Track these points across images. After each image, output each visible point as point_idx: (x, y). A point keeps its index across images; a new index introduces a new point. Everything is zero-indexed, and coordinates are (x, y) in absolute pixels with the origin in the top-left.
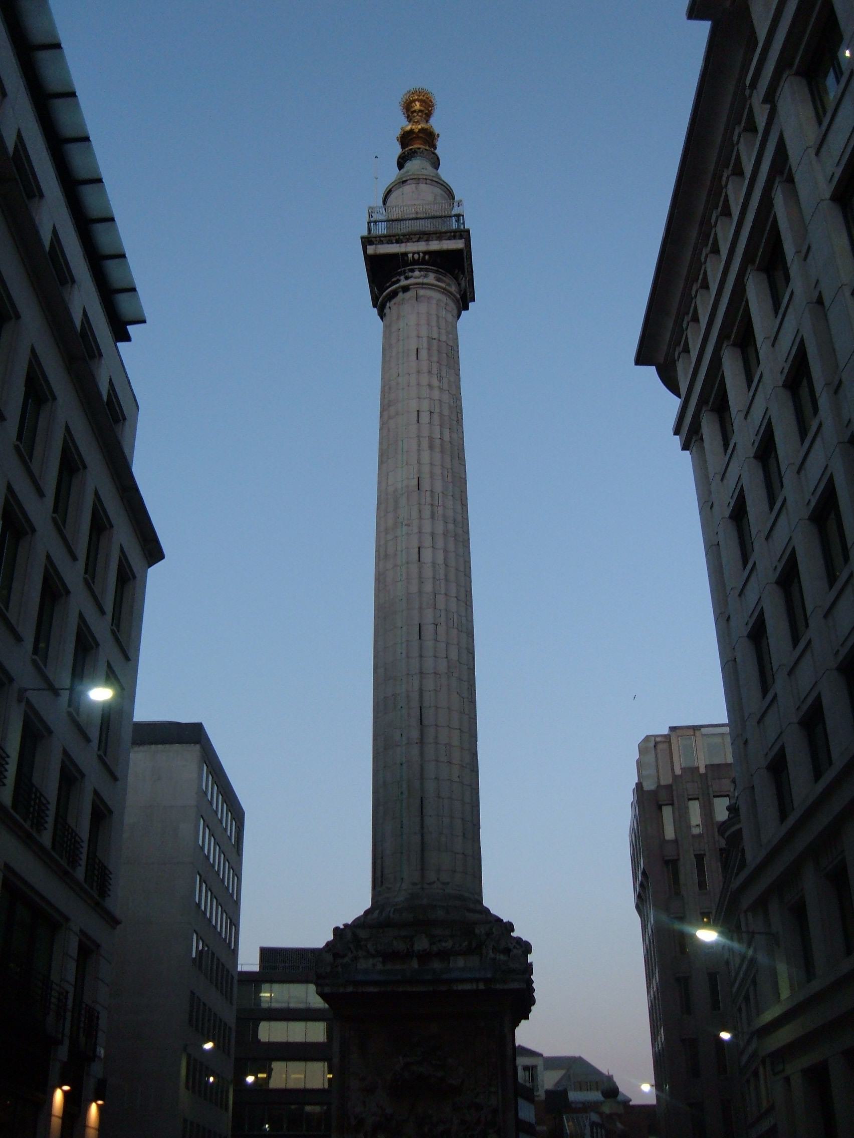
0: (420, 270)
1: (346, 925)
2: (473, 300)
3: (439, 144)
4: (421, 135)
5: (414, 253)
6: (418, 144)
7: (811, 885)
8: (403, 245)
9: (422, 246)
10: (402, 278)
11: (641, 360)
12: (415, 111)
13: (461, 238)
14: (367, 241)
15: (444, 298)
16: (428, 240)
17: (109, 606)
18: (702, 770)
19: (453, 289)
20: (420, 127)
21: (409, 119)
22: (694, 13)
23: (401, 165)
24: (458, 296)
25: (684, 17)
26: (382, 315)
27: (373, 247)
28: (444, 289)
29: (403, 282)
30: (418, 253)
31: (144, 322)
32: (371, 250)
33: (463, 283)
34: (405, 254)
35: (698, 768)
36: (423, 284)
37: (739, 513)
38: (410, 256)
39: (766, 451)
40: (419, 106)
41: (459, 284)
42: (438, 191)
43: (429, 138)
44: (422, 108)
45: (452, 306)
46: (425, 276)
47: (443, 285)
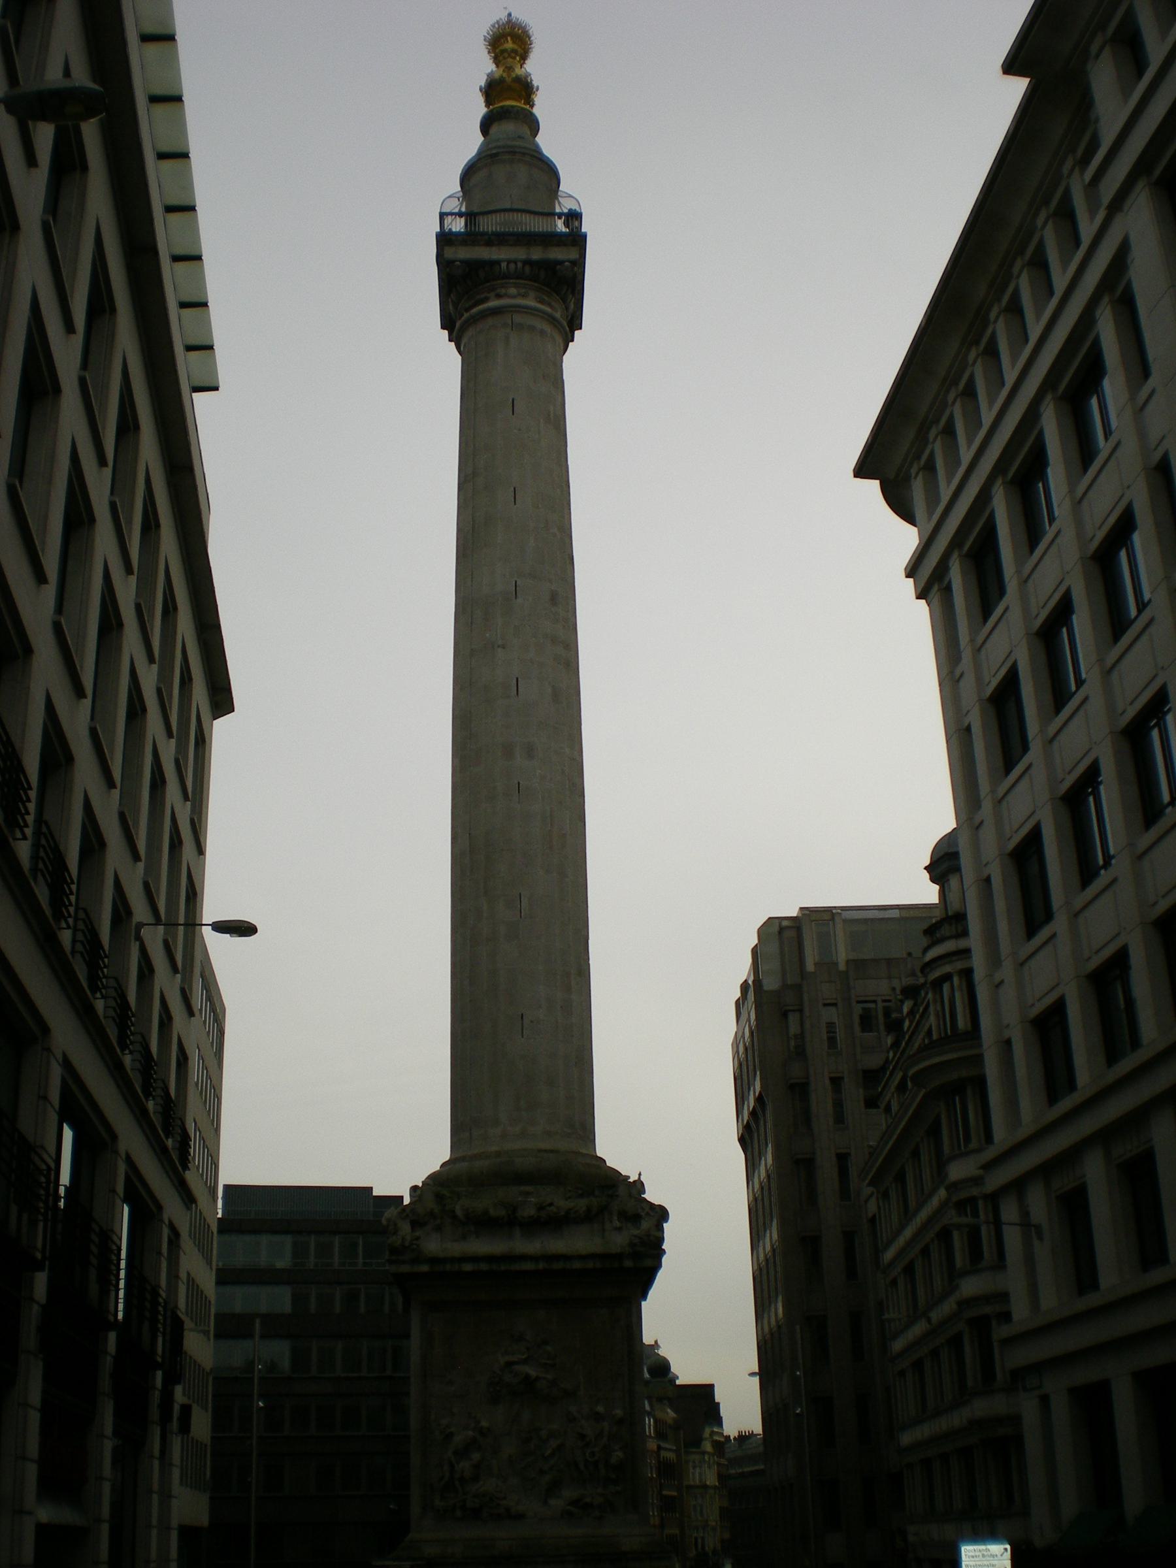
0: (516, 286)
5: (509, 262)
7: (1095, 1172)
9: (519, 253)
10: (492, 295)
11: (863, 470)
14: (445, 239)
15: (548, 328)
18: (842, 967)
21: (497, 60)
22: (1011, 67)
29: (493, 303)
31: (216, 389)
32: (450, 253)
35: (836, 964)
36: (519, 306)
37: (1004, 698)
38: (504, 265)
39: (1051, 631)
40: (510, 42)
41: (567, 308)
43: (526, 90)
44: (515, 47)
46: (524, 296)
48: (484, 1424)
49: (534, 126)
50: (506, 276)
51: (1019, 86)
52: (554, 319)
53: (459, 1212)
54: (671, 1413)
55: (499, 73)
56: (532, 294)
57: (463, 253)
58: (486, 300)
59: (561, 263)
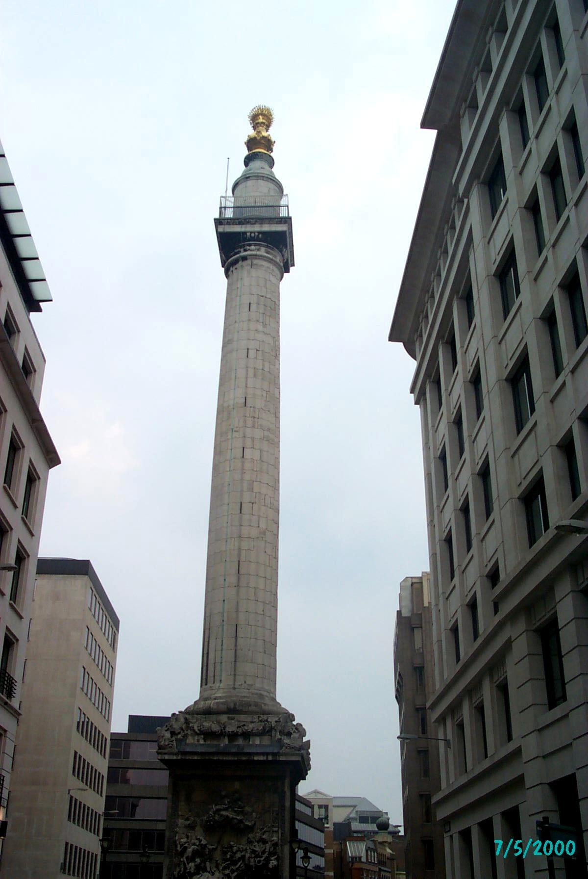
0: (255, 245)
1: (180, 712)
2: (293, 265)
3: (275, 148)
6: (259, 149)
11: (393, 338)
13: (285, 222)
14: (218, 222)
15: (271, 266)
16: (261, 223)
17: (20, 502)
19: (278, 259)
21: (254, 128)
22: (425, 124)
23: (246, 164)
24: (282, 264)
25: (419, 126)
26: (227, 276)
29: (243, 254)
32: (221, 229)
33: (286, 255)
34: (245, 233)
36: (256, 255)
40: (261, 119)
42: (272, 186)
43: (268, 144)
45: (277, 271)
48: (204, 842)
49: (271, 163)
51: (432, 134)
53: (196, 728)
54: (389, 851)
56: (263, 249)
58: (240, 252)
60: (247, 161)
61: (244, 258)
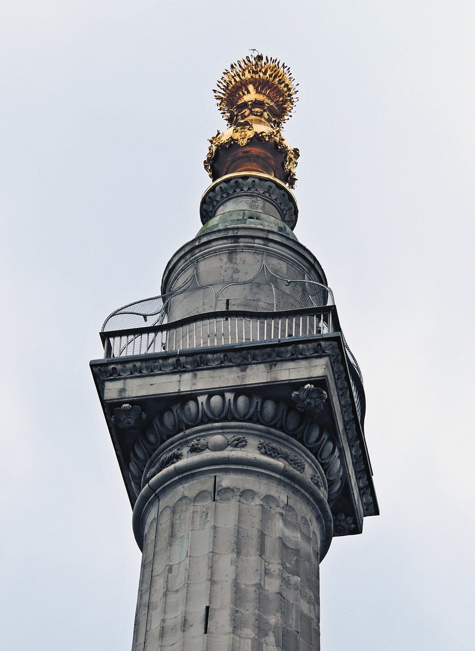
4: (255, 150)
5: (211, 394)
8: (187, 377)
9: (228, 378)
10: (185, 450)
12: (245, 105)
14: (102, 372)
16: (243, 365)
20: (250, 134)
24: (323, 494)
27: (118, 385)
28: (284, 473)
30: (221, 392)
32: (113, 389)
38: (202, 399)
41: (326, 467)
47: (280, 463)
50: (205, 418)
52: (292, 478)
55: (227, 133)
56: (253, 442)
57: (138, 388)
58: (178, 457)
59: (297, 385)
60: (208, 208)
61: (187, 474)
